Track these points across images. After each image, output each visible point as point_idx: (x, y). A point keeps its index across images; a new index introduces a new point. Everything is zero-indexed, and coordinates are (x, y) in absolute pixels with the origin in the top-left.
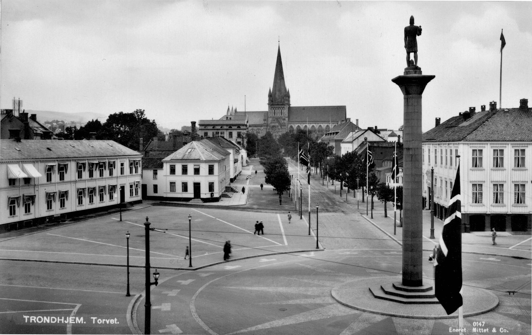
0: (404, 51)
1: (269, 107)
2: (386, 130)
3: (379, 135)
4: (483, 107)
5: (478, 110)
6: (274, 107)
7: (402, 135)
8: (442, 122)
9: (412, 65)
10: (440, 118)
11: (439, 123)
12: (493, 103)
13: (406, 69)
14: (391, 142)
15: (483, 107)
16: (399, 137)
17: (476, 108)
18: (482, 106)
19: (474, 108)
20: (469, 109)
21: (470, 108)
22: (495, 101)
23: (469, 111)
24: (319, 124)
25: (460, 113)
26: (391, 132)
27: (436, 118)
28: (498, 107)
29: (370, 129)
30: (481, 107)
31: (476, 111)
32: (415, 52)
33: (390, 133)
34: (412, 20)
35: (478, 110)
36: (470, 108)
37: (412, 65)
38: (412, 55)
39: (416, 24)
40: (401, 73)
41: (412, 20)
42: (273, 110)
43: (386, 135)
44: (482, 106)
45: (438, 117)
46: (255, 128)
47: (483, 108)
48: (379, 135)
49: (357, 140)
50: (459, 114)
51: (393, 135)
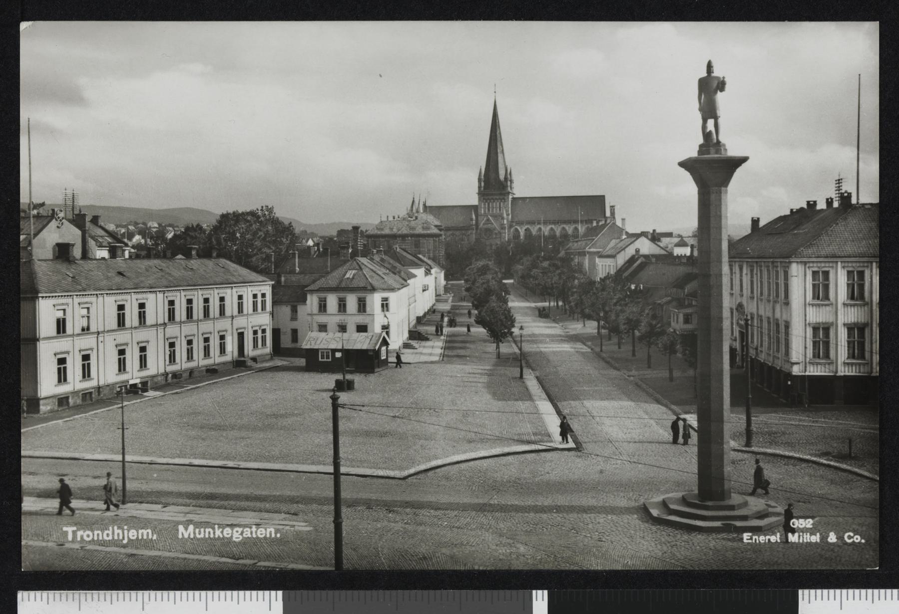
0: (698, 116)
1: (479, 198)
2: (669, 235)
3: (659, 243)
4: (830, 200)
5: (821, 205)
6: (488, 199)
7: (697, 244)
8: (762, 224)
9: (710, 142)
10: (758, 219)
11: (758, 225)
12: (846, 195)
13: (701, 146)
14: (679, 255)
15: (830, 200)
16: (692, 247)
17: (817, 202)
18: (827, 199)
19: (815, 202)
20: (806, 203)
21: (808, 202)
22: (849, 191)
23: (805, 207)
24: (562, 226)
25: (792, 210)
26: (680, 239)
27: (752, 218)
28: (854, 201)
29: (644, 234)
30: (825, 201)
31: (819, 207)
32: (716, 118)
33: (676, 240)
34: (710, 67)
35: (821, 205)
36: (808, 202)
37: (710, 142)
38: (711, 123)
39: (717, 73)
40: (694, 154)
41: (710, 67)
42: (487, 204)
43: (671, 243)
44: (827, 199)
45: (756, 216)
46: (457, 233)
47: (829, 202)
48: (659, 243)
49: (623, 252)
50: (789, 211)
51: (682, 244)
